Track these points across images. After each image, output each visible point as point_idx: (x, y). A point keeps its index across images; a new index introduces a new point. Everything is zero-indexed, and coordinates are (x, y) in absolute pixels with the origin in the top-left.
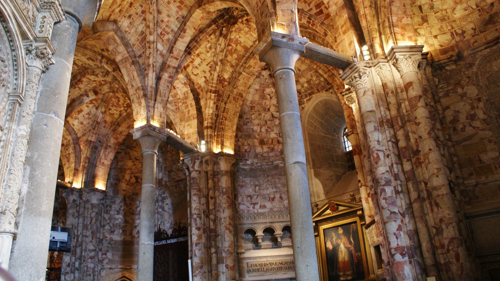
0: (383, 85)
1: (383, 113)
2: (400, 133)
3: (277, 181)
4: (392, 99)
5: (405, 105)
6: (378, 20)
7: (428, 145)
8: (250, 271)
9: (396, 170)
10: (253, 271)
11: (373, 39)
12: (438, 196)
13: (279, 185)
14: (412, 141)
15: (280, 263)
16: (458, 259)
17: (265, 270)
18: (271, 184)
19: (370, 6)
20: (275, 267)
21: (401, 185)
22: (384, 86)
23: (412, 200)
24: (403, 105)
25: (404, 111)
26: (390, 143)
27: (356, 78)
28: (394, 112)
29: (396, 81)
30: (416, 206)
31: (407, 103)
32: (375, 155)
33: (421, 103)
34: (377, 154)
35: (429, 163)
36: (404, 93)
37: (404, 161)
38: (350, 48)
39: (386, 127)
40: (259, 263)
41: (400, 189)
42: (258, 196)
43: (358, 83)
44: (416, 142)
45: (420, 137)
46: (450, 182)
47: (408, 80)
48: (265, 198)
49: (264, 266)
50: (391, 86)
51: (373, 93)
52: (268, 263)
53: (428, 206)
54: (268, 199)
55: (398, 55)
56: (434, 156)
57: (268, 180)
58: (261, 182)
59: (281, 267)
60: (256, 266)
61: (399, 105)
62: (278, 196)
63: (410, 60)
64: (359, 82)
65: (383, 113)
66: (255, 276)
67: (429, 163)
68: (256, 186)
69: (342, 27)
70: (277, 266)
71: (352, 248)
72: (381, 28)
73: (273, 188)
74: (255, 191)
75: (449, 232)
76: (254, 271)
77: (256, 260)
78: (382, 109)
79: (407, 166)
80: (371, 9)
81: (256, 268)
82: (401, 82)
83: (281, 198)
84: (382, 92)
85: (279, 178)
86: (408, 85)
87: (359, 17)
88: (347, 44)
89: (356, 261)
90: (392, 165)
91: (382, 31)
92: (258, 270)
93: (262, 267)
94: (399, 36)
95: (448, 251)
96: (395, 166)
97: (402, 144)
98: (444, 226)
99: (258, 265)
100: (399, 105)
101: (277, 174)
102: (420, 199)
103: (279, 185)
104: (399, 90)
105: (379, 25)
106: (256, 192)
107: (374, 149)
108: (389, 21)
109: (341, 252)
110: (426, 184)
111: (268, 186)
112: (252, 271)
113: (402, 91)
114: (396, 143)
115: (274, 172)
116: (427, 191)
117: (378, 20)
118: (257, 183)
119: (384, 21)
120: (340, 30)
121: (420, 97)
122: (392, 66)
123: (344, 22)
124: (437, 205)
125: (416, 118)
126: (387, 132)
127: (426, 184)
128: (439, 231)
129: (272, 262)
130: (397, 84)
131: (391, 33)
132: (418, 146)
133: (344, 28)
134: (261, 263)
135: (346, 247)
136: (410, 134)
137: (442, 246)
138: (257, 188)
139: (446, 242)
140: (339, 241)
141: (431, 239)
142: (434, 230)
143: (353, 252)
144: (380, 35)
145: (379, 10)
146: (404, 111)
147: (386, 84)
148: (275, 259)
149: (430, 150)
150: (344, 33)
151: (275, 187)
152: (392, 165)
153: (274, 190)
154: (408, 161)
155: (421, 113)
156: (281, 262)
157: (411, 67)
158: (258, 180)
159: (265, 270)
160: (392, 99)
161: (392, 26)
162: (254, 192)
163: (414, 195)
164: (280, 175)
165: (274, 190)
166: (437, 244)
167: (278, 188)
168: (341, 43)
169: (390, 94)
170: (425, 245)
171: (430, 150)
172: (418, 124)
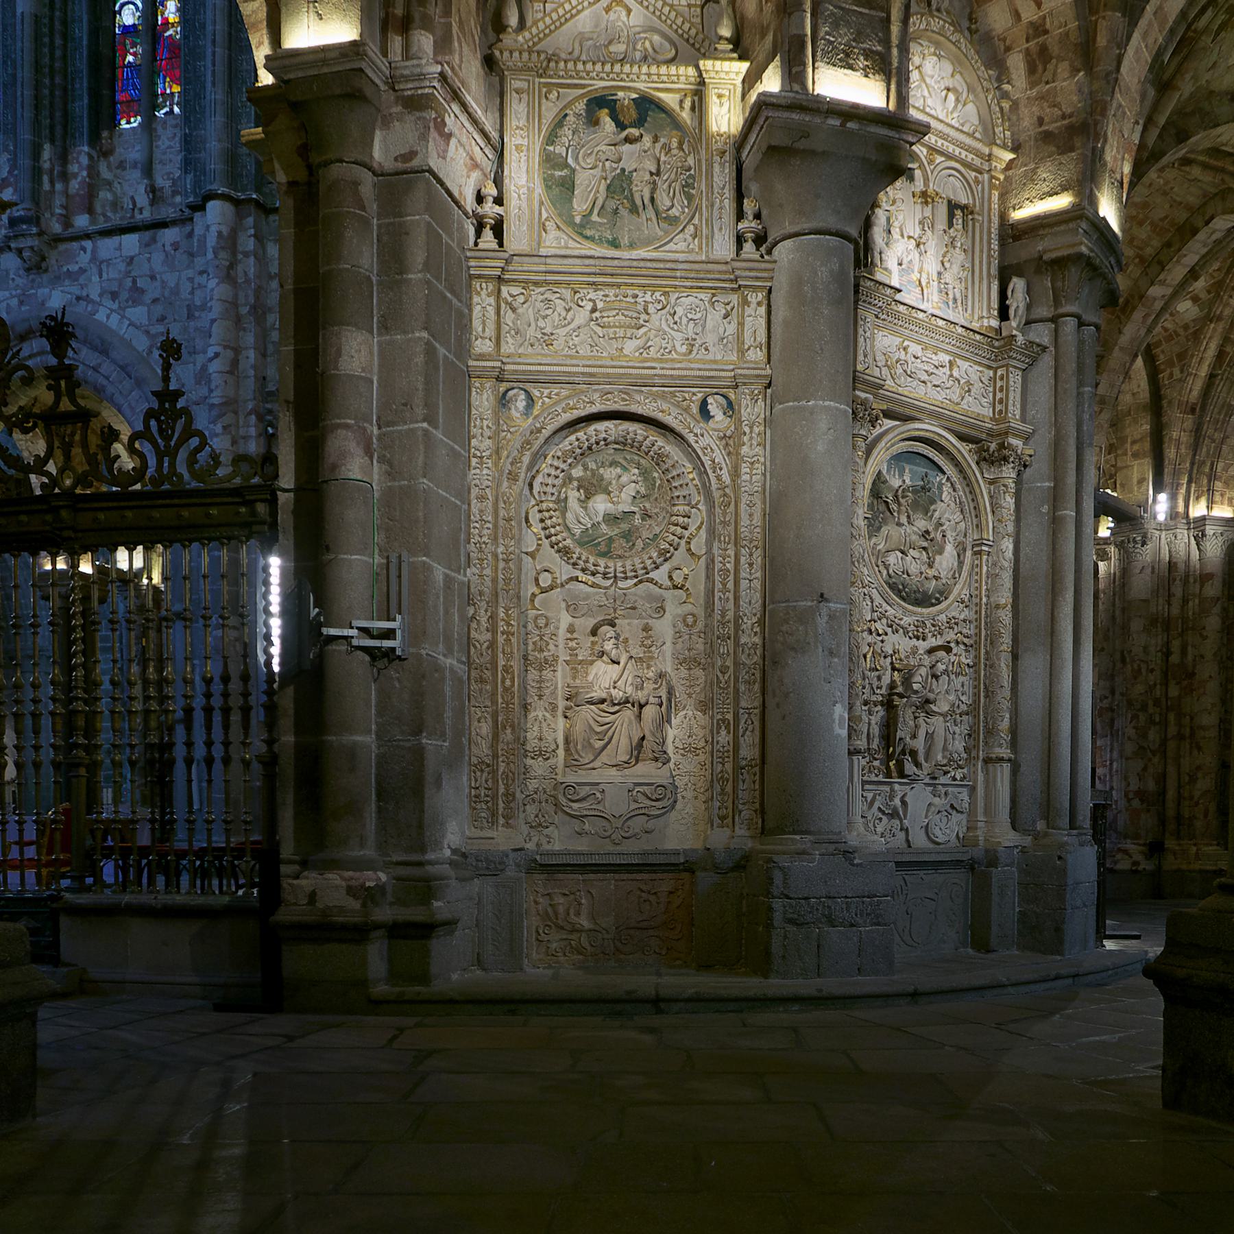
0: (1169, 562)
1: (1160, 608)
2: (1176, 645)
4: (1178, 591)
5: (1193, 604)
6: (1194, 455)
7: (1208, 671)
9: (1158, 693)
11: (1177, 486)
12: (1204, 738)
14: (1190, 657)
16: (1206, 816)
19: (1191, 431)
21: (1160, 714)
22: (1172, 565)
23: (1169, 736)
24: (1191, 604)
25: (1190, 613)
26: (1159, 654)
27: (1135, 542)
28: (1175, 611)
29: (1192, 564)
30: (1172, 745)
31: (1197, 601)
32: (1136, 666)
33: (1217, 609)
34: (1139, 666)
35: (1204, 693)
36: (1198, 586)
37: (1172, 683)
38: (1140, 488)
39: (1160, 629)
41: (1157, 720)
43: (1138, 550)
44: (1194, 660)
45: (1202, 657)
46: (1221, 721)
47: (1209, 569)
50: (1181, 566)
51: (1153, 572)
53: (1188, 746)
55: (1210, 530)
56: (1213, 687)
61: (1185, 601)
63: (1220, 539)
64: (1138, 550)
65: (1160, 608)
67: (1204, 693)
69: (1134, 442)
72: (1195, 471)
75: (1205, 784)
78: (1161, 601)
79: (1174, 691)
80: (1190, 436)
82: (1198, 566)
84: (1167, 574)
86: (1205, 578)
87: (1166, 439)
88: (1135, 481)
90: (1155, 685)
91: (1194, 476)
94: (1217, 497)
95: (1197, 804)
96: (1158, 687)
97: (1175, 658)
98: (1200, 775)
100: (1185, 601)
102: (1180, 737)
104: (1192, 580)
105: (1192, 464)
107: (1136, 658)
108: (1212, 469)
110: (1192, 719)
113: (1195, 582)
114: (1167, 654)
116: (1191, 728)
117: (1194, 455)
119: (1204, 462)
120: (1128, 446)
121: (1218, 599)
122: (1192, 538)
123: (1139, 436)
124: (1199, 749)
125: (1204, 628)
126: (1160, 637)
127: (1192, 719)
128: (1193, 779)
130: (1192, 569)
131: (1209, 490)
132: (1194, 666)
133: (1136, 447)
136: (1190, 648)
137: (1191, 798)
139: (1197, 794)
141: (1180, 787)
142: (1187, 779)
144: (1190, 482)
145: (1201, 440)
146: (1190, 613)
147: (1175, 563)
149: (1210, 677)
150: (1136, 455)
152: (1155, 685)
154: (1177, 684)
155: (1213, 622)
157: (1219, 549)
160: (1178, 591)
161: (1212, 477)
163: (1172, 730)
166: (1186, 794)
168: (1125, 471)
169: (1178, 582)
170: (1171, 794)
171: (1210, 677)
172: (1205, 638)
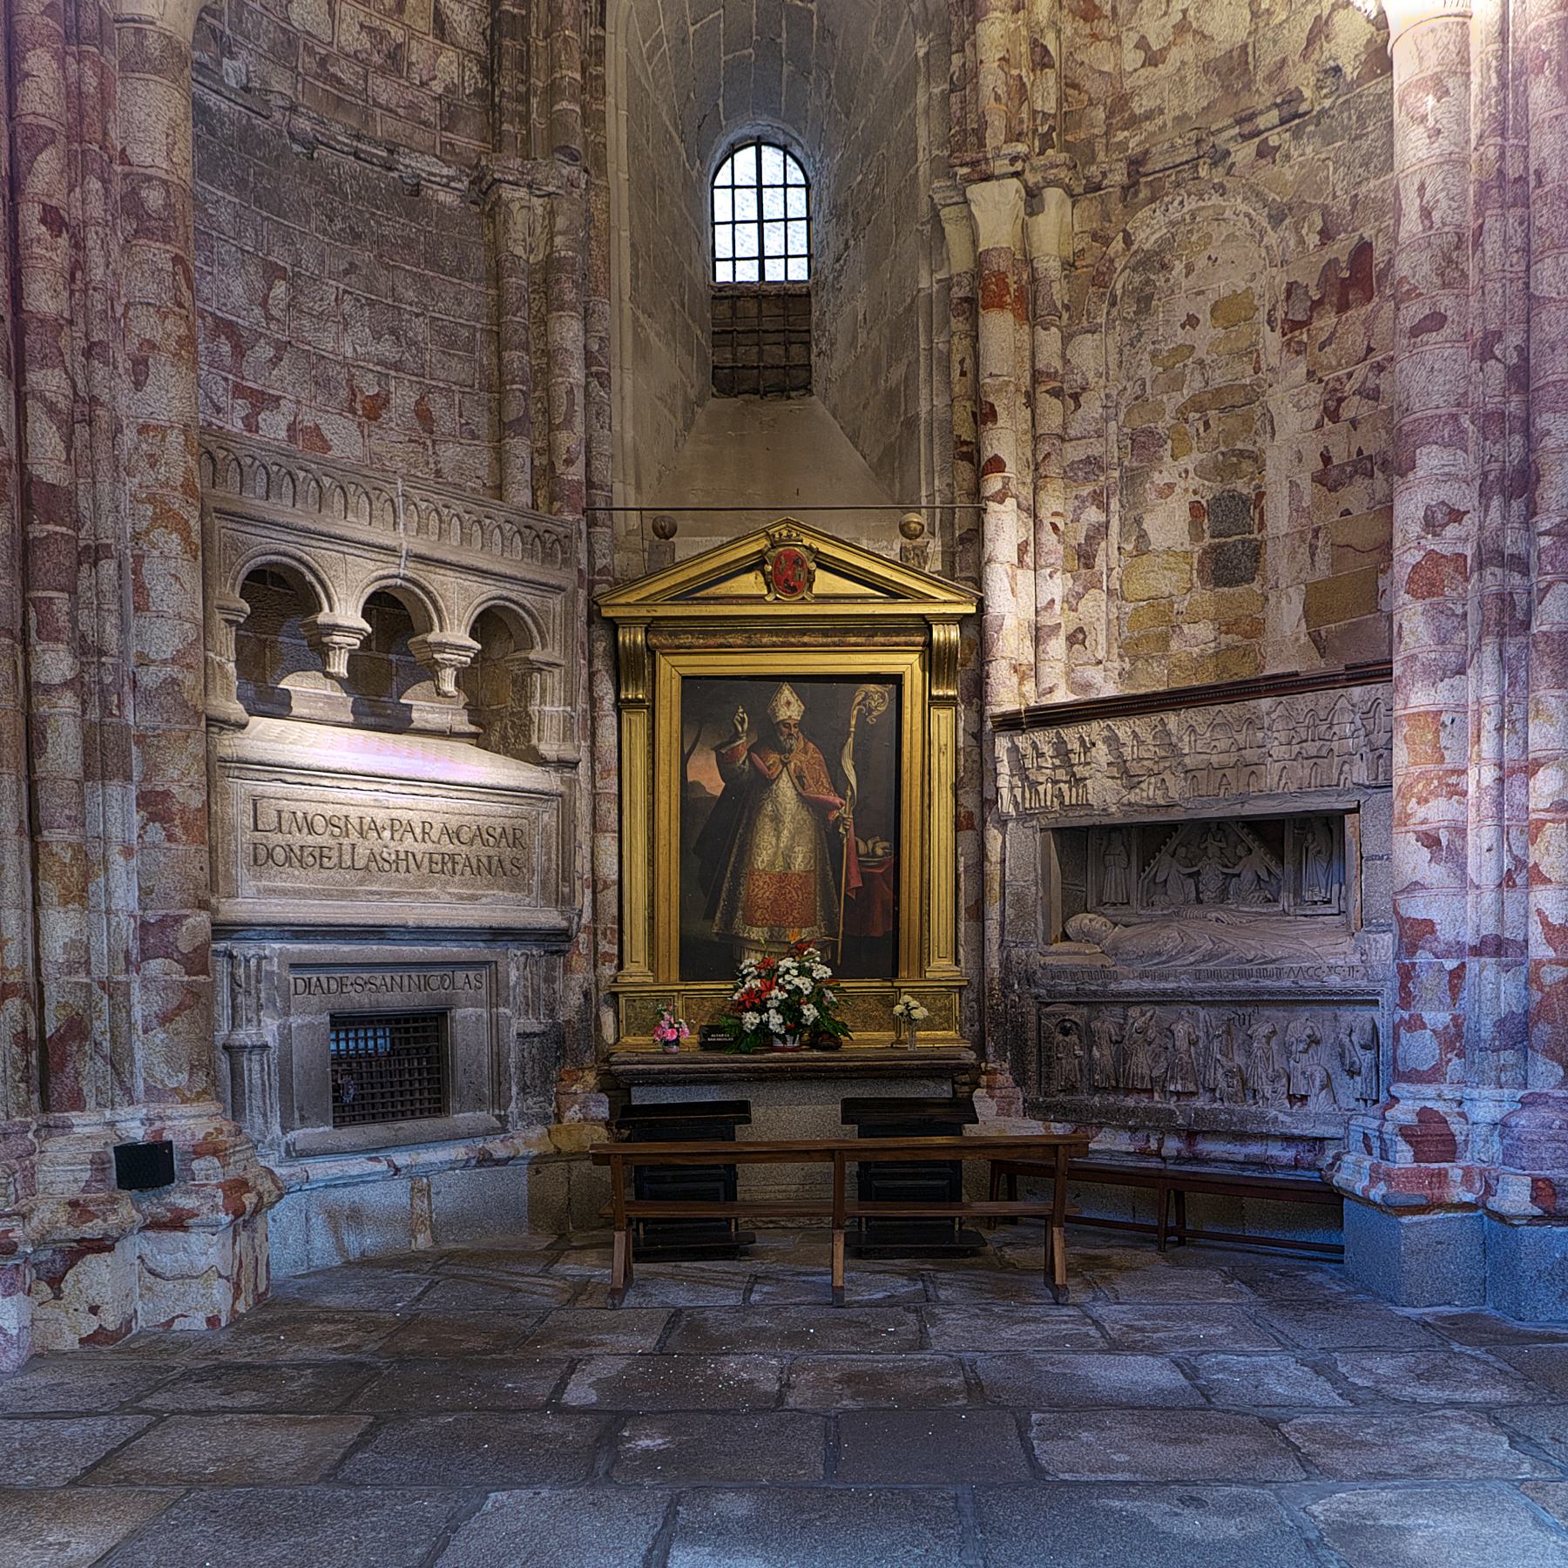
3: (410, 295)
8: (270, 855)
10: (288, 859)
13: (420, 329)
15: (445, 830)
17: (360, 864)
18: (371, 303)
20: (418, 848)
40: (329, 810)
42: (281, 347)
48: (322, 383)
49: (354, 836)
52: (381, 816)
54: (344, 393)
57: (352, 268)
58: (310, 263)
59: (452, 856)
60: (311, 829)
62: (403, 397)
66: (299, 893)
68: (273, 272)
70: (429, 846)
71: (846, 812)
73: (378, 337)
74: (264, 304)
76: (295, 857)
77: (312, 792)
81: (310, 840)
83: (423, 415)
85: (425, 285)
89: (856, 882)
92: (321, 854)
93: (345, 841)
99: (319, 823)
101: (408, 244)
103: (420, 329)
106: (269, 318)
109: (777, 819)
111: (347, 307)
112: (280, 855)
115: (394, 227)
118: (279, 257)
129: (405, 815)
134: (344, 810)
135: (804, 800)
138: (280, 289)
140: (774, 758)
143: (847, 831)
148: (422, 803)
151: (393, 332)
153: (387, 349)
156: (453, 823)
158: (287, 239)
159: (360, 864)
162: (257, 311)
164: (432, 262)
165: (387, 349)
167: (413, 343)
